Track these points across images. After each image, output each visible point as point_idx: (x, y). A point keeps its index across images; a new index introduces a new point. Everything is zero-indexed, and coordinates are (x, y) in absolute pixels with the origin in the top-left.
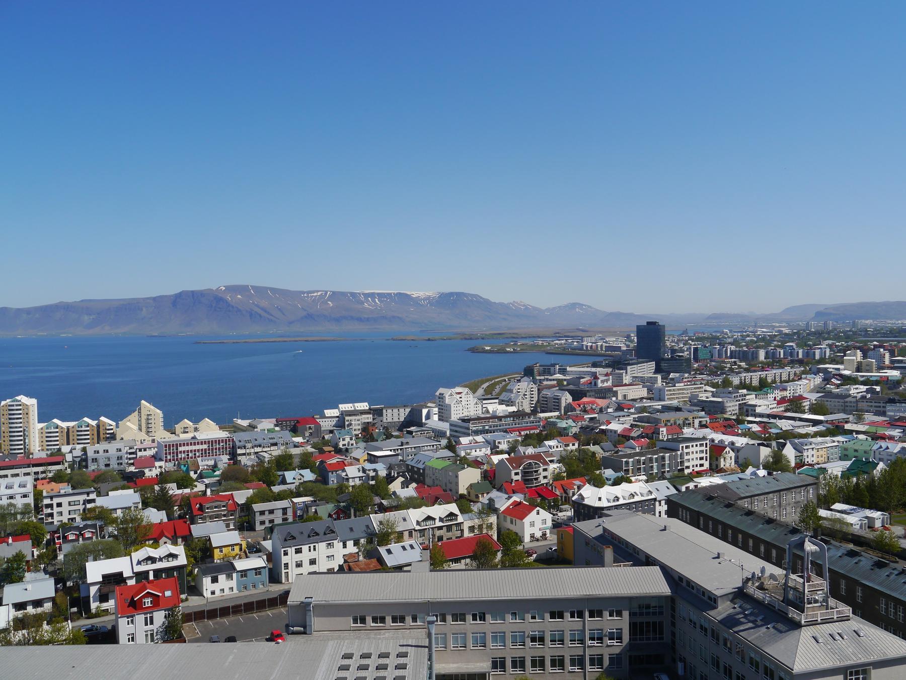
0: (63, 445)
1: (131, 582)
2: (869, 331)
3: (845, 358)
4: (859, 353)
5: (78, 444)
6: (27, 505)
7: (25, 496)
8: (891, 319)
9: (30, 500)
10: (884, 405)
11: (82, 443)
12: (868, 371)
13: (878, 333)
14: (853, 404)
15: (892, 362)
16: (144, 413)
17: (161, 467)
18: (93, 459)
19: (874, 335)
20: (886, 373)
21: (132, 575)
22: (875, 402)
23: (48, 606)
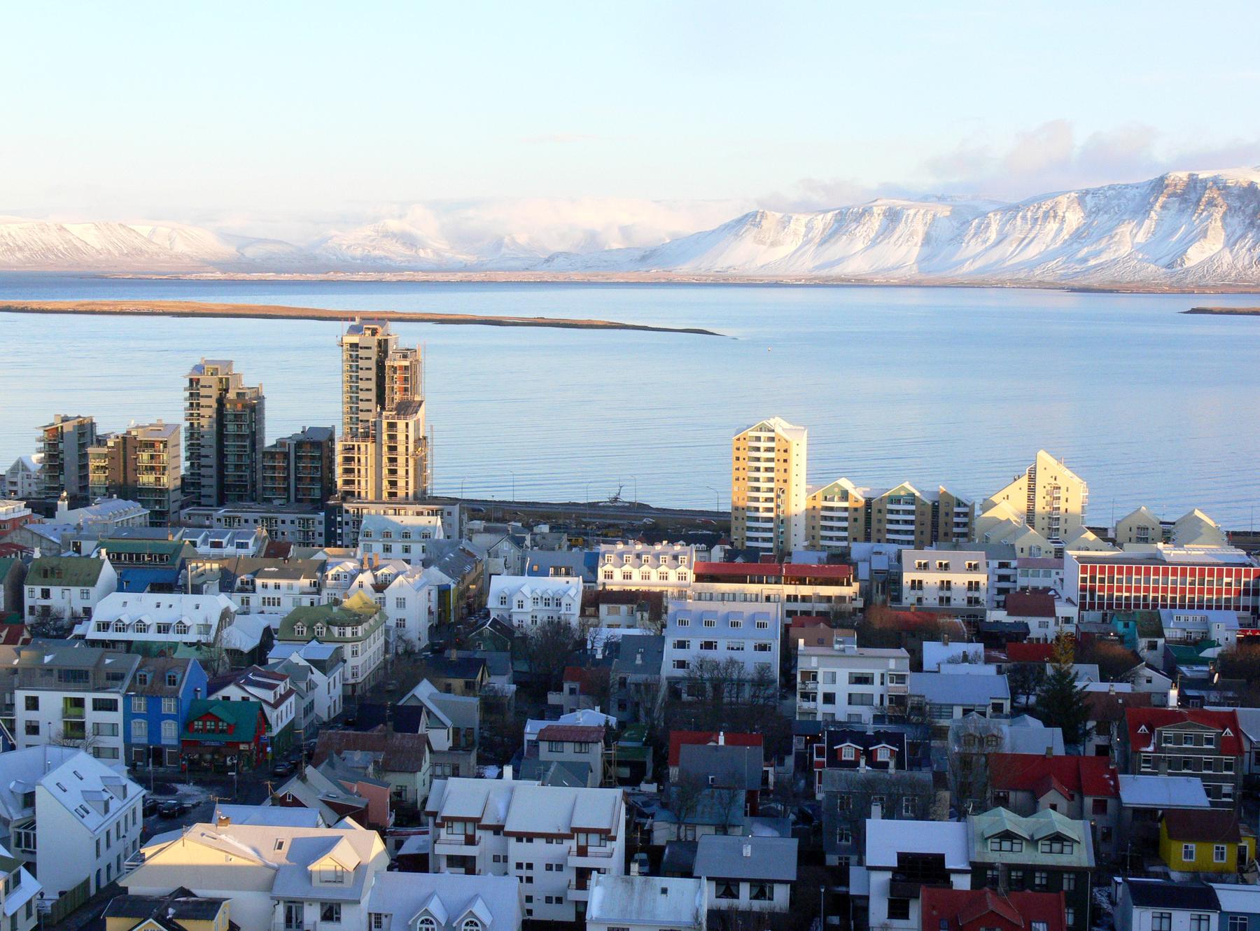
0: (855, 540)
1: (962, 883)
5: (888, 541)
6: (764, 669)
7: (763, 648)
9: (773, 658)
11: (894, 541)
16: (1042, 480)
17: (1068, 620)
18: (913, 582)
21: (964, 866)
23: (781, 896)
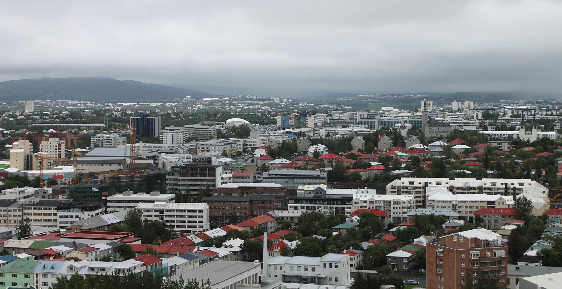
2: (46, 114)
3: (11, 151)
4: (28, 144)
8: (72, 99)
10: (55, 211)
12: (41, 167)
13: (56, 118)
14: (18, 213)
15: (69, 155)
19: (52, 119)
20: (61, 169)
22: (45, 209)
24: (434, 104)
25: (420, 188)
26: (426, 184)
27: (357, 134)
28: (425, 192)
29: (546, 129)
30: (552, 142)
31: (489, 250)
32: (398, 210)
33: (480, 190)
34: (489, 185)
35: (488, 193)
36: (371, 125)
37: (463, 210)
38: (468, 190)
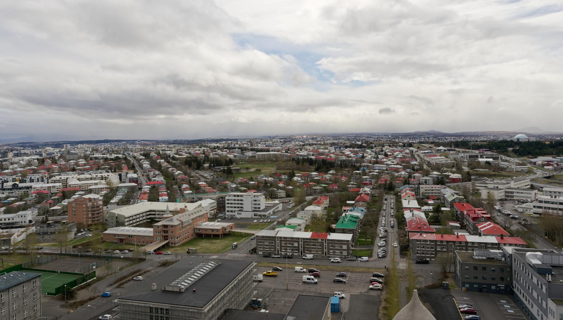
24: (70, 146)
25: (64, 180)
26: (67, 178)
27: (34, 159)
28: (67, 181)
29: (117, 154)
30: (120, 158)
31: (95, 202)
32: (54, 190)
33: (91, 179)
34: (95, 177)
35: (94, 180)
36: (41, 155)
37: (84, 187)
38: (87, 179)
